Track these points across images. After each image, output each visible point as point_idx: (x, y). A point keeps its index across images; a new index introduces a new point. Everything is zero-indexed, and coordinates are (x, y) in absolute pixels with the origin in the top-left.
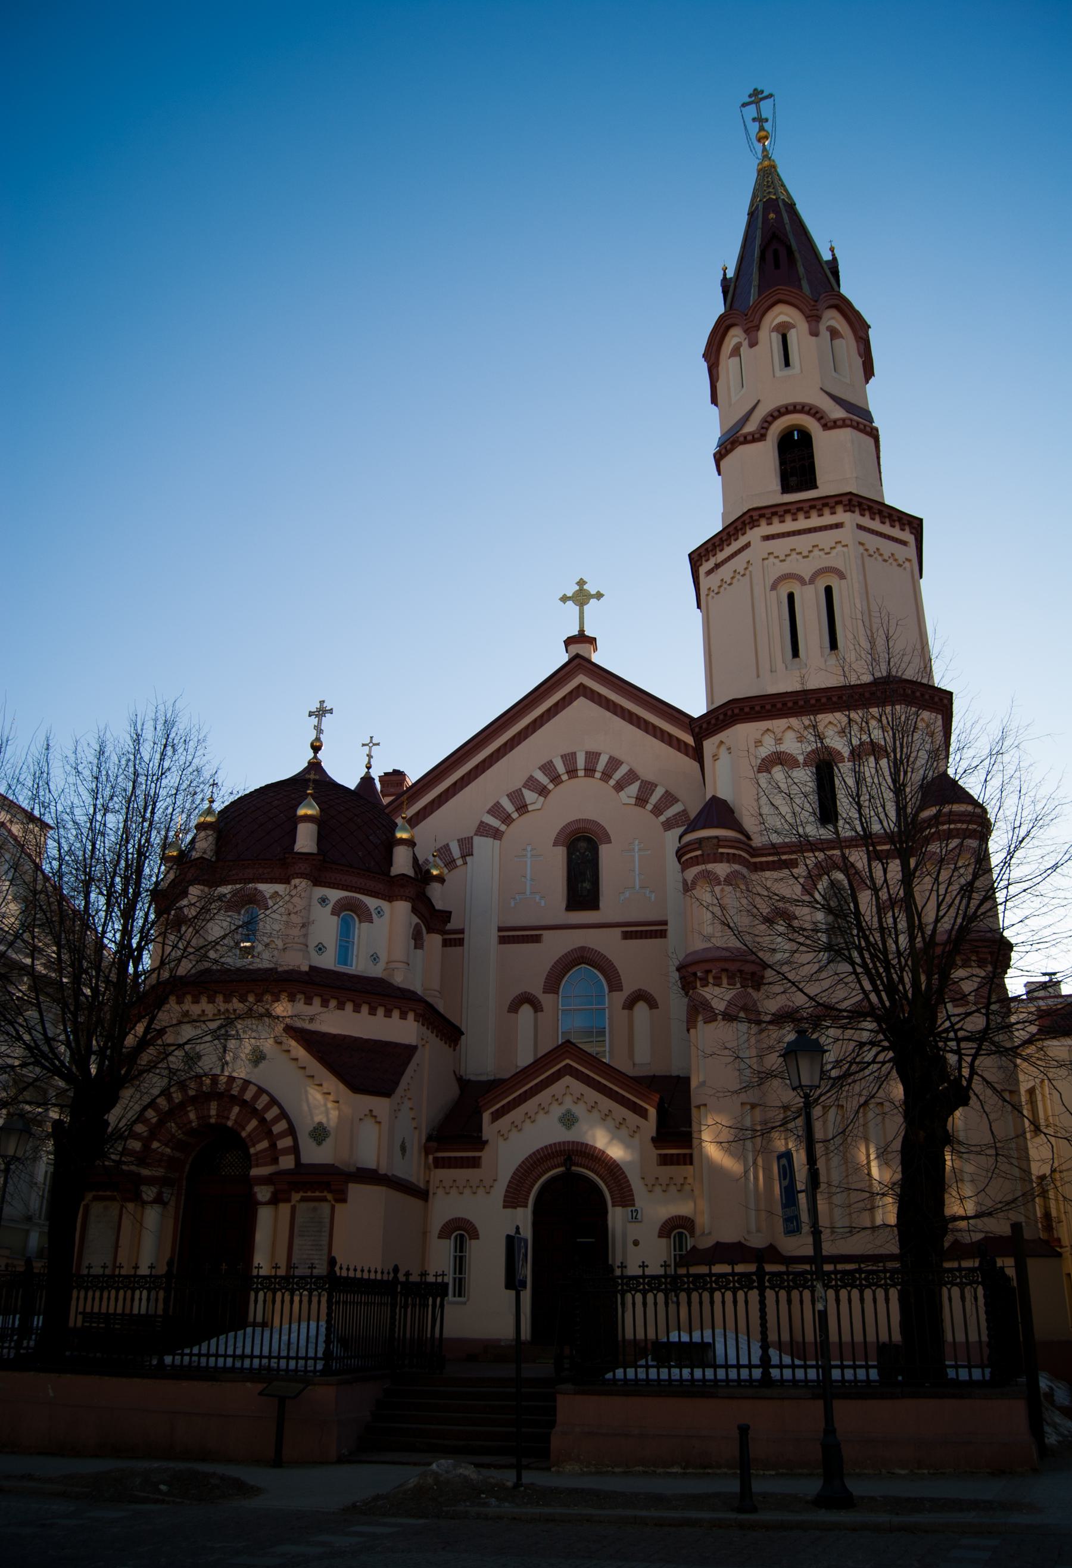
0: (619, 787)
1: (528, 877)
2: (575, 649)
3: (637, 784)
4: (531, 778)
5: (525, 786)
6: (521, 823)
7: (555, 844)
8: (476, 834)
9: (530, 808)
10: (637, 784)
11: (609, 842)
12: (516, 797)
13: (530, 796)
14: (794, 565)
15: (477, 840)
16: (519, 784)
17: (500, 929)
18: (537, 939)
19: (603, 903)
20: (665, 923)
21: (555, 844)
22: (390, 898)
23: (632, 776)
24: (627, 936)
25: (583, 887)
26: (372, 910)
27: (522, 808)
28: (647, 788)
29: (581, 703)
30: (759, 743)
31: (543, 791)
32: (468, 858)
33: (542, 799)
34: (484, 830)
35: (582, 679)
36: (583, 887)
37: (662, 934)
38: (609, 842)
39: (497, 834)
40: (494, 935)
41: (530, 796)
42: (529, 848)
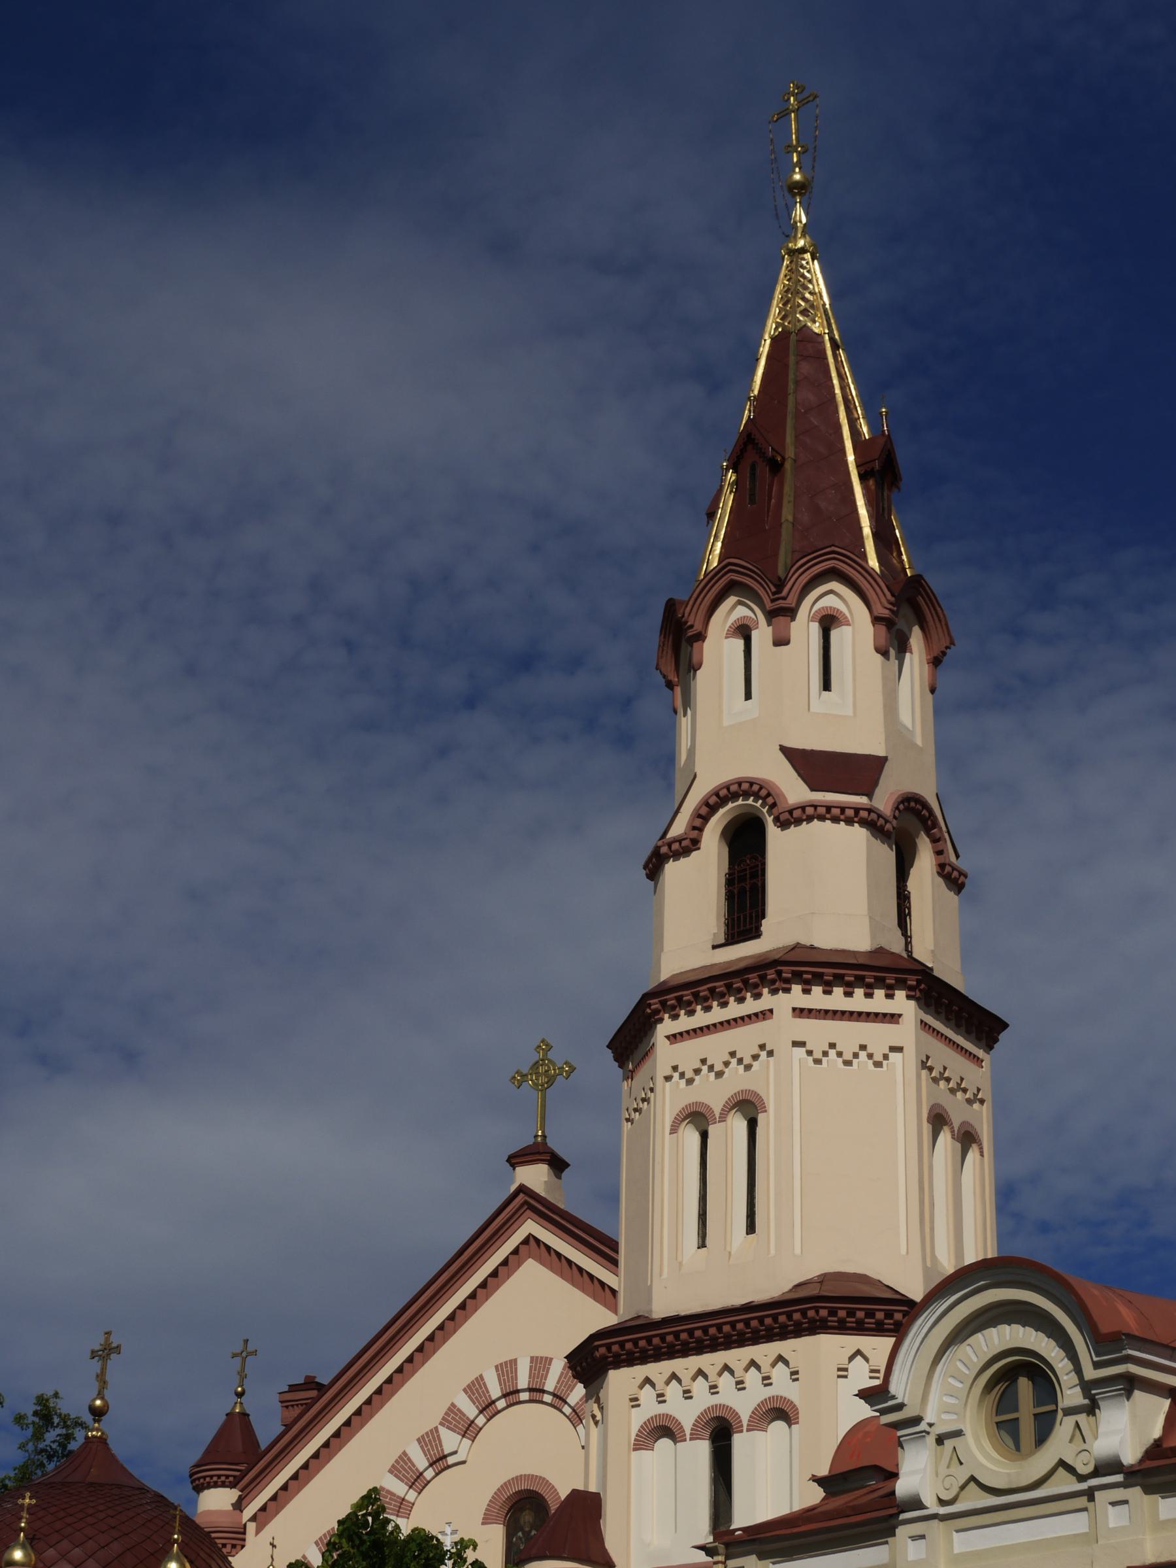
5: (445, 1422)
6: (441, 1485)
7: (486, 1521)
9: (451, 1460)
12: (429, 1440)
13: (450, 1440)
16: (434, 1420)
21: (486, 1521)
27: (440, 1462)
31: (469, 1430)
35: (531, 1227)
41: (450, 1440)
42: (448, 1530)
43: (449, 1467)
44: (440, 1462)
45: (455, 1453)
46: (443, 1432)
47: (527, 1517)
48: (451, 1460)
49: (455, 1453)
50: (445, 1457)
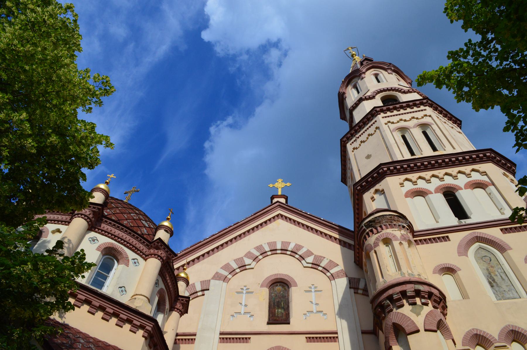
0: (302, 258)
1: (243, 304)
2: (275, 200)
3: (313, 256)
4: (249, 252)
5: (246, 256)
7: (262, 286)
8: (212, 279)
9: (247, 267)
10: (313, 256)
11: (296, 285)
14: (402, 124)
15: (213, 282)
17: (221, 334)
18: (247, 340)
19: (292, 320)
20: (337, 333)
21: (262, 286)
22: (145, 257)
23: (309, 253)
24: (309, 340)
25: (279, 312)
26: (130, 259)
28: (319, 258)
29: (280, 221)
30: (402, 185)
31: (255, 259)
32: (206, 292)
33: (254, 263)
34: (217, 277)
35: (280, 211)
36: (279, 312)
37: (335, 339)
38: (296, 285)
39: (225, 279)
40: (217, 336)
41: (247, 261)
42: (245, 289)
43: (246, 269)
44: (243, 267)
45: (250, 265)
46: (244, 258)
47: (278, 288)
48: (247, 267)
49: (250, 265)
50: (245, 266)
